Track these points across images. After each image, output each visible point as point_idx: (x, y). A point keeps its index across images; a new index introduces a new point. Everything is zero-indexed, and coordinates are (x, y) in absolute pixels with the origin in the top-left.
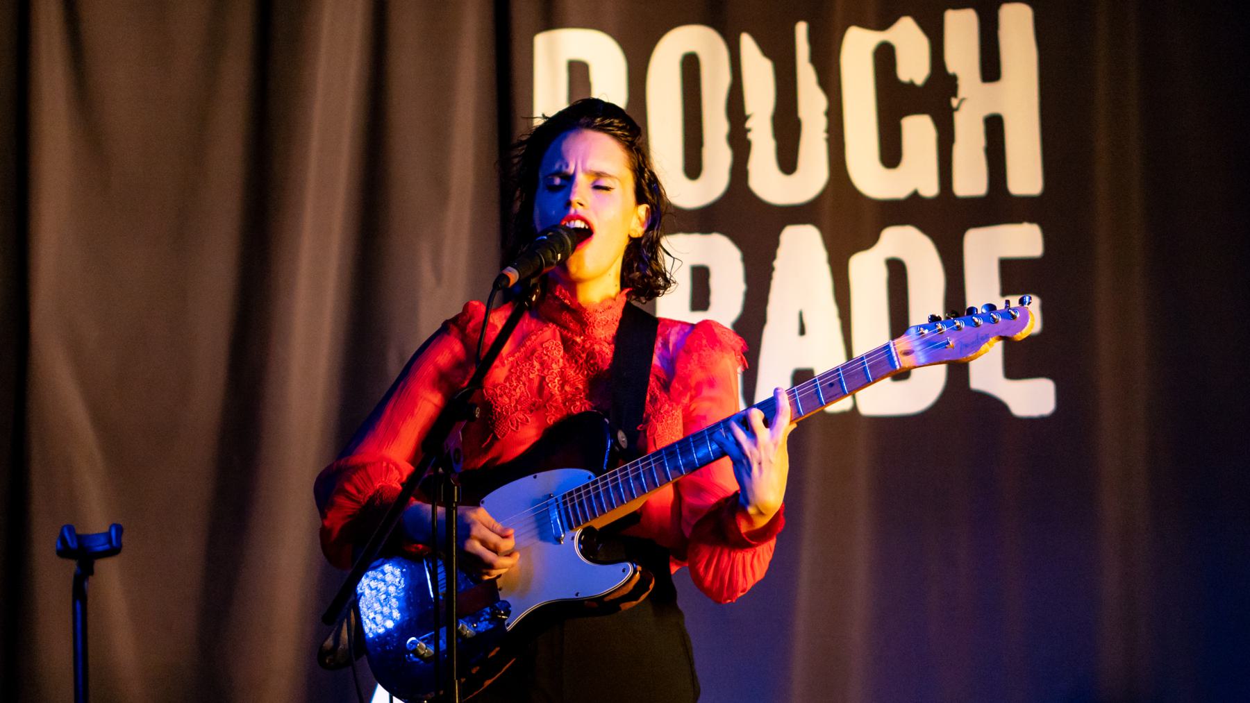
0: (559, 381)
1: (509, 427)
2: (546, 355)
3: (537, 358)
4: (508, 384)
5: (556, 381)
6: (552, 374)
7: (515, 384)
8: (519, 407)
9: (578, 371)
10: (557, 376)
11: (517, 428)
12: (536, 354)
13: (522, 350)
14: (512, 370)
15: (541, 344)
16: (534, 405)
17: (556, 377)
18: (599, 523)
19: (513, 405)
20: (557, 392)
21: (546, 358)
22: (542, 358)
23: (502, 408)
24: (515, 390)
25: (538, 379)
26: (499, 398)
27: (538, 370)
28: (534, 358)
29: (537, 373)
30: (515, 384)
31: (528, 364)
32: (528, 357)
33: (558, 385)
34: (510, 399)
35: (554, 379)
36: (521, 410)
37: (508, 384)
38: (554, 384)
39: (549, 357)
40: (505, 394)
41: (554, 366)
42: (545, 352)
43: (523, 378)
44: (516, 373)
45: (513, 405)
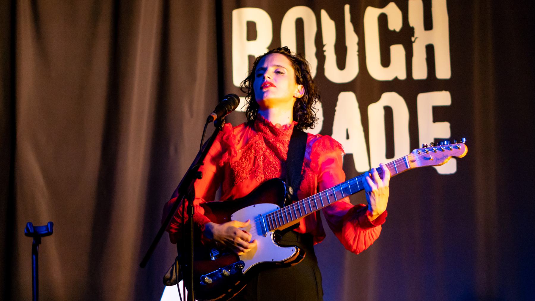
1: (239, 180)
2: (257, 147)
3: (253, 148)
6: (259, 155)
7: (244, 161)
8: (245, 171)
9: (270, 154)
10: (262, 156)
11: (243, 180)
12: (253, 147)
13: (247, 145)
16: (251, 171)
18: (281, 228)
19: (242, 170)
21: (257, 148)
22: (255, 148)
23: (237, 172)
24: (243, 163)
25: (254, 157)
27: (254, 154)
28: (252, 148)
29: (253, 155)
30: (244, 161)
31: (249, 151)
32: (249, 149)
37: (240, 161)
39: (258, 147)
40: (239, 165)
41: (260, 151)
42: (257, 145)
45: (242, 170)
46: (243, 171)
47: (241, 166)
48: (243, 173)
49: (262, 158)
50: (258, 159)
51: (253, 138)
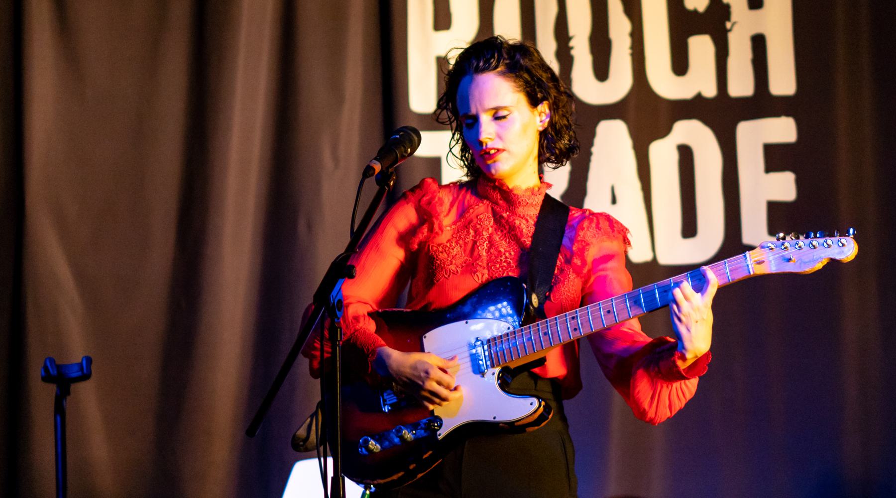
0: (487, 244)
2: (480, 224)
4: (448, 245)
5: (485, 244)
6: (482, 239)
8: (454, 262)
10: (486, 241)
13: (462, 220)
14: (454, 236)
15: (477, 217)
16: (465, 263)
17: (485, 242)
19: (449, 259)
20: (484, 254)
22: (476, 227)
23: (441, 261)
24: (453, 249)
26: (440, 254)
29: (471, 238)
30: (454, 245)
31: (465, 231)
33: (486, 248)
34: (448, 255)
35: (484, 243)
36: (455, 264)
37: (448, 245)
38: (483, 247)
40: (445, 251)
41: (484, 233)
42: (479, 222)
43: (461, 242)
44: (456, 238)
45: (449, 259)
46: (451, 262)
47: (449, 254)
48: (451, 264)
49: (487, 246)
50: (479, 246)
51: (473, 208)
